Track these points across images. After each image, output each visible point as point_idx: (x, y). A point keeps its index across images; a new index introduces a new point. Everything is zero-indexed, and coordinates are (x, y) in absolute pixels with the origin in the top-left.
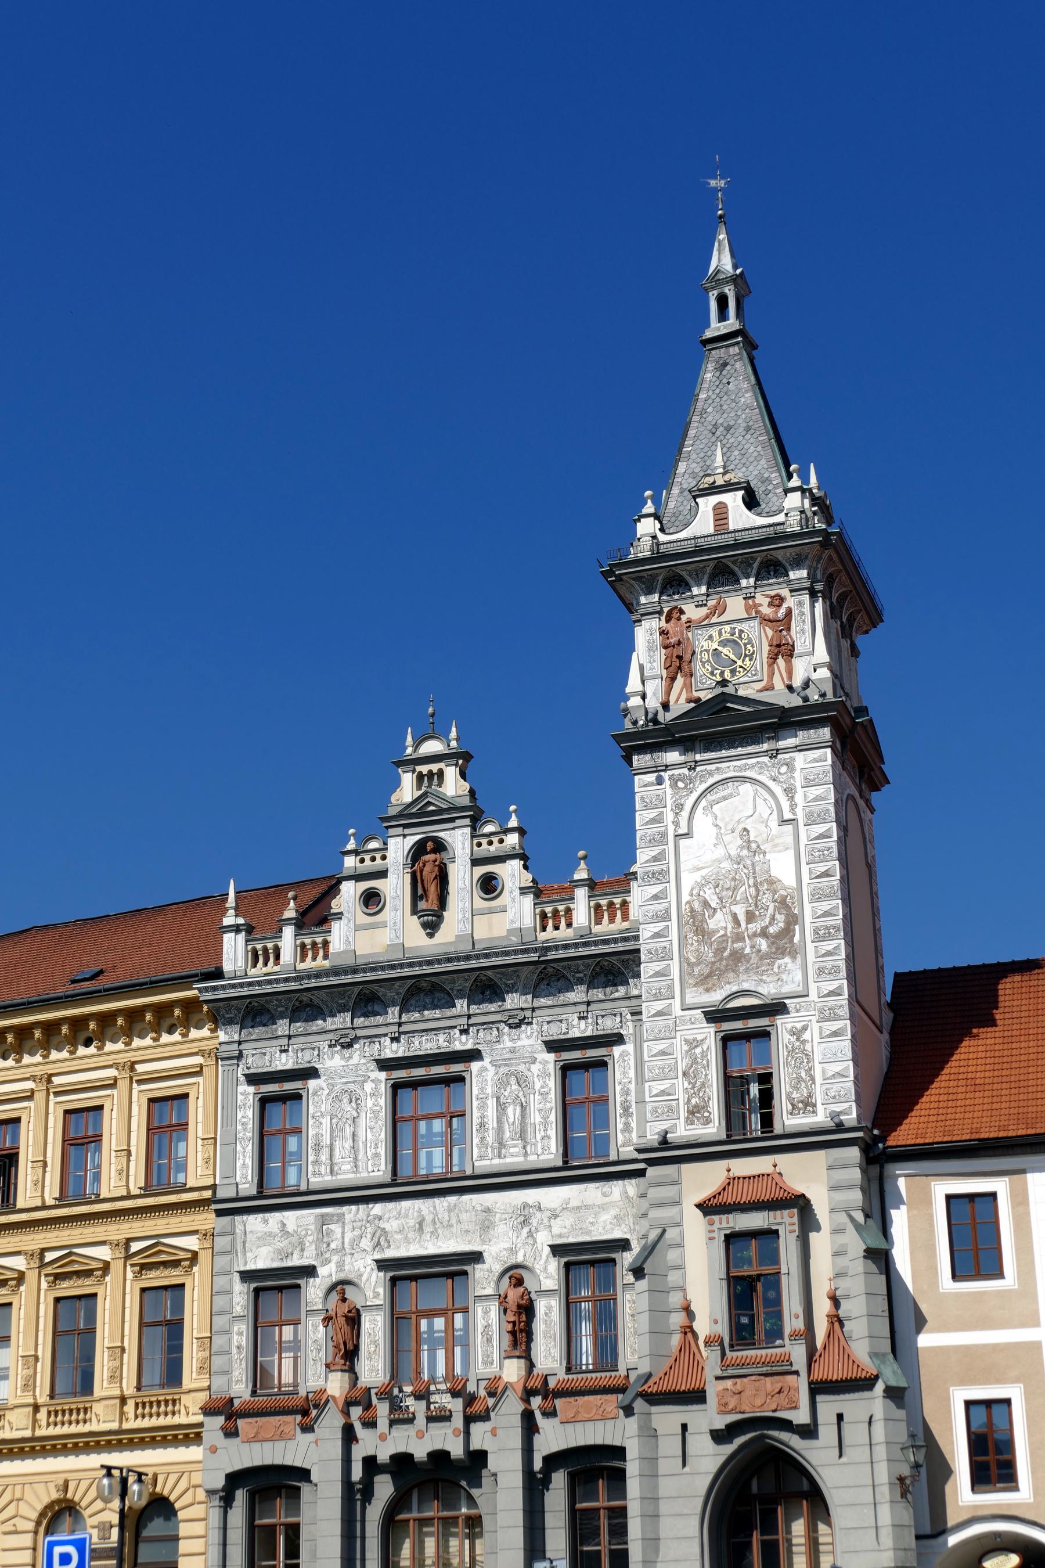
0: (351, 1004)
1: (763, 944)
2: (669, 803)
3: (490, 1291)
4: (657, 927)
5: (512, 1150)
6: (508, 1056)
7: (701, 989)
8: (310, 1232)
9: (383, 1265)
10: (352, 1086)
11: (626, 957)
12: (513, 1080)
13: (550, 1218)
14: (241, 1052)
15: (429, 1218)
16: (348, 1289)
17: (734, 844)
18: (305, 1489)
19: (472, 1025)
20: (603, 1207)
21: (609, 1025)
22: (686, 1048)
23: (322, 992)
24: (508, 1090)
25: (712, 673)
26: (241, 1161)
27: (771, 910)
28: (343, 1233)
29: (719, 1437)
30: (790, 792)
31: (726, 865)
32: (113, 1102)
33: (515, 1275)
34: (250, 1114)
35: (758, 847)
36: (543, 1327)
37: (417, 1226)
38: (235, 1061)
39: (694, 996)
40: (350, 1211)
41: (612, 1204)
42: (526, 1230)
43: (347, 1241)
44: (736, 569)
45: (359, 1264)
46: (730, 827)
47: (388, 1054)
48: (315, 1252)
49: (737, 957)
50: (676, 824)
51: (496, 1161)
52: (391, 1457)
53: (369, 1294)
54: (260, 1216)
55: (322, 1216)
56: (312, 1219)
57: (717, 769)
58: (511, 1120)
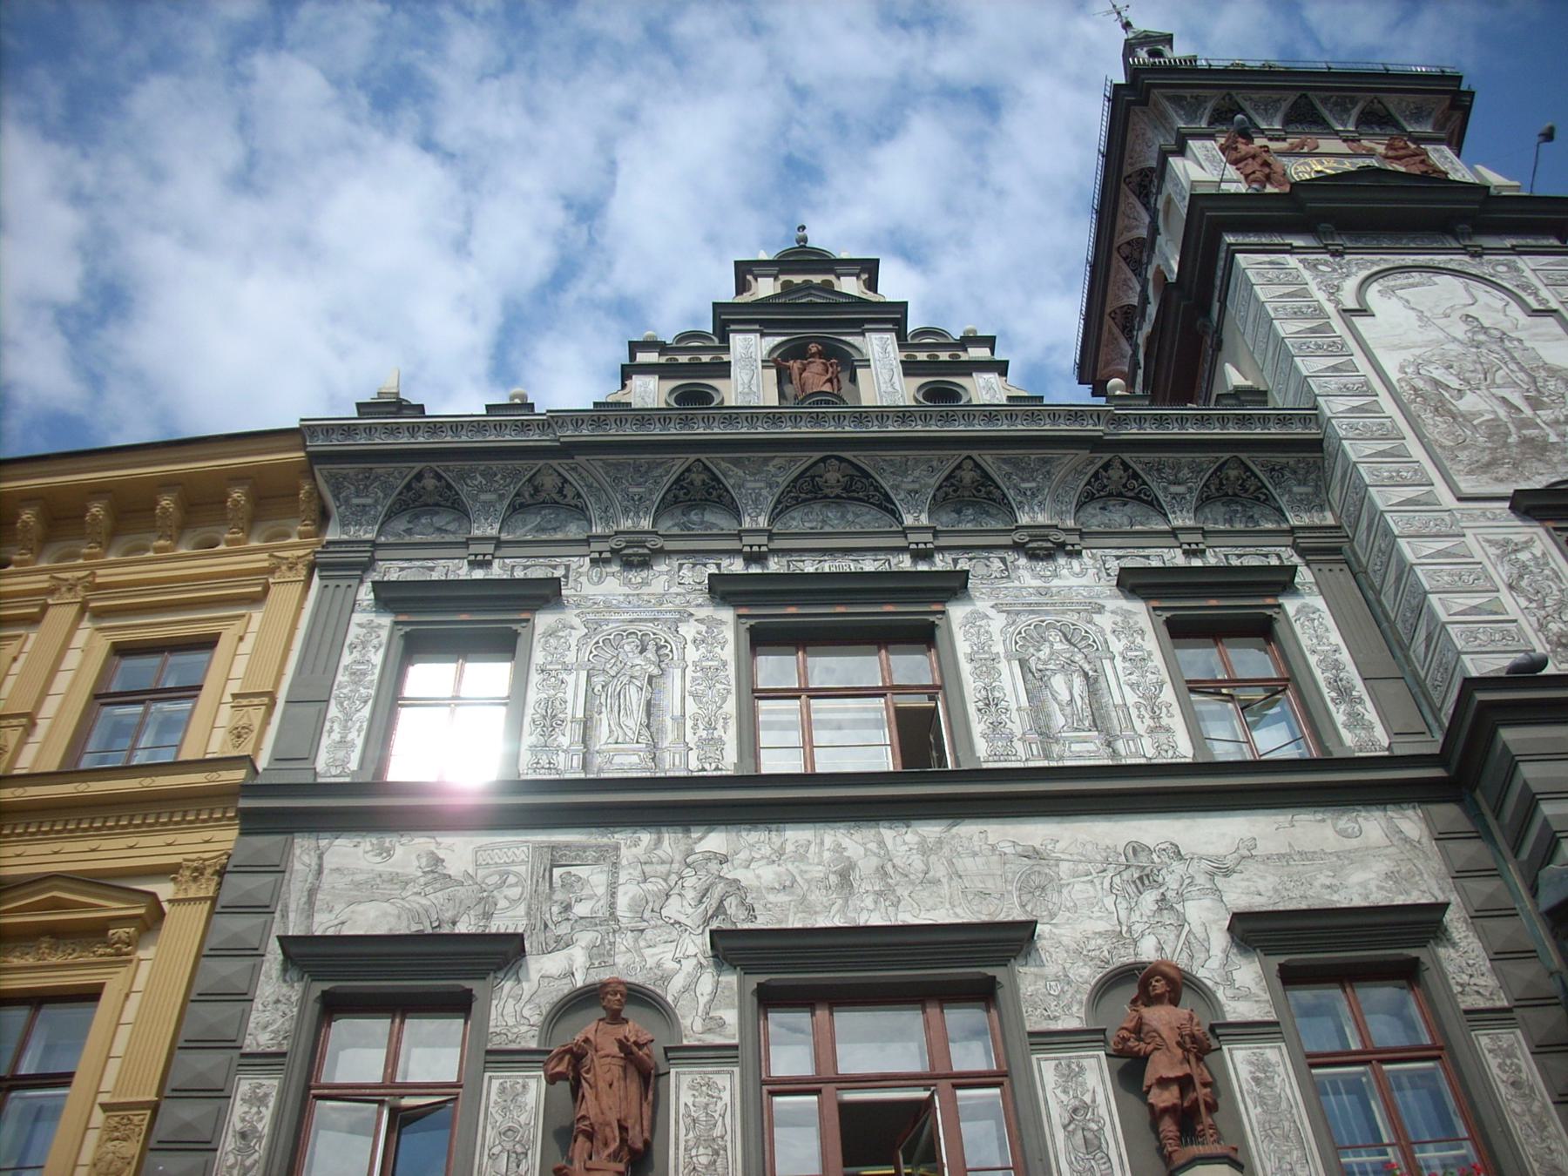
0: (657, 497)
6: (1034, 599)
7: (1485, 478)
8: (512, 879)
10: (648, 627)
11: (1280, 458)
12: (1054, 636)
13: (1212, 875)
19: (941, 549)
20: (1346, 858)
22: (1492, 551)
23: (595, 463)
26: (336, 736)
34: (377, 658)
36: (1255, 1112)
37: (833, 879)
40: (635, 844)
42: (1149, 898)
43: (623, 902)
55: (553, 848)
56: (522, 853)
58: (1065, 697)
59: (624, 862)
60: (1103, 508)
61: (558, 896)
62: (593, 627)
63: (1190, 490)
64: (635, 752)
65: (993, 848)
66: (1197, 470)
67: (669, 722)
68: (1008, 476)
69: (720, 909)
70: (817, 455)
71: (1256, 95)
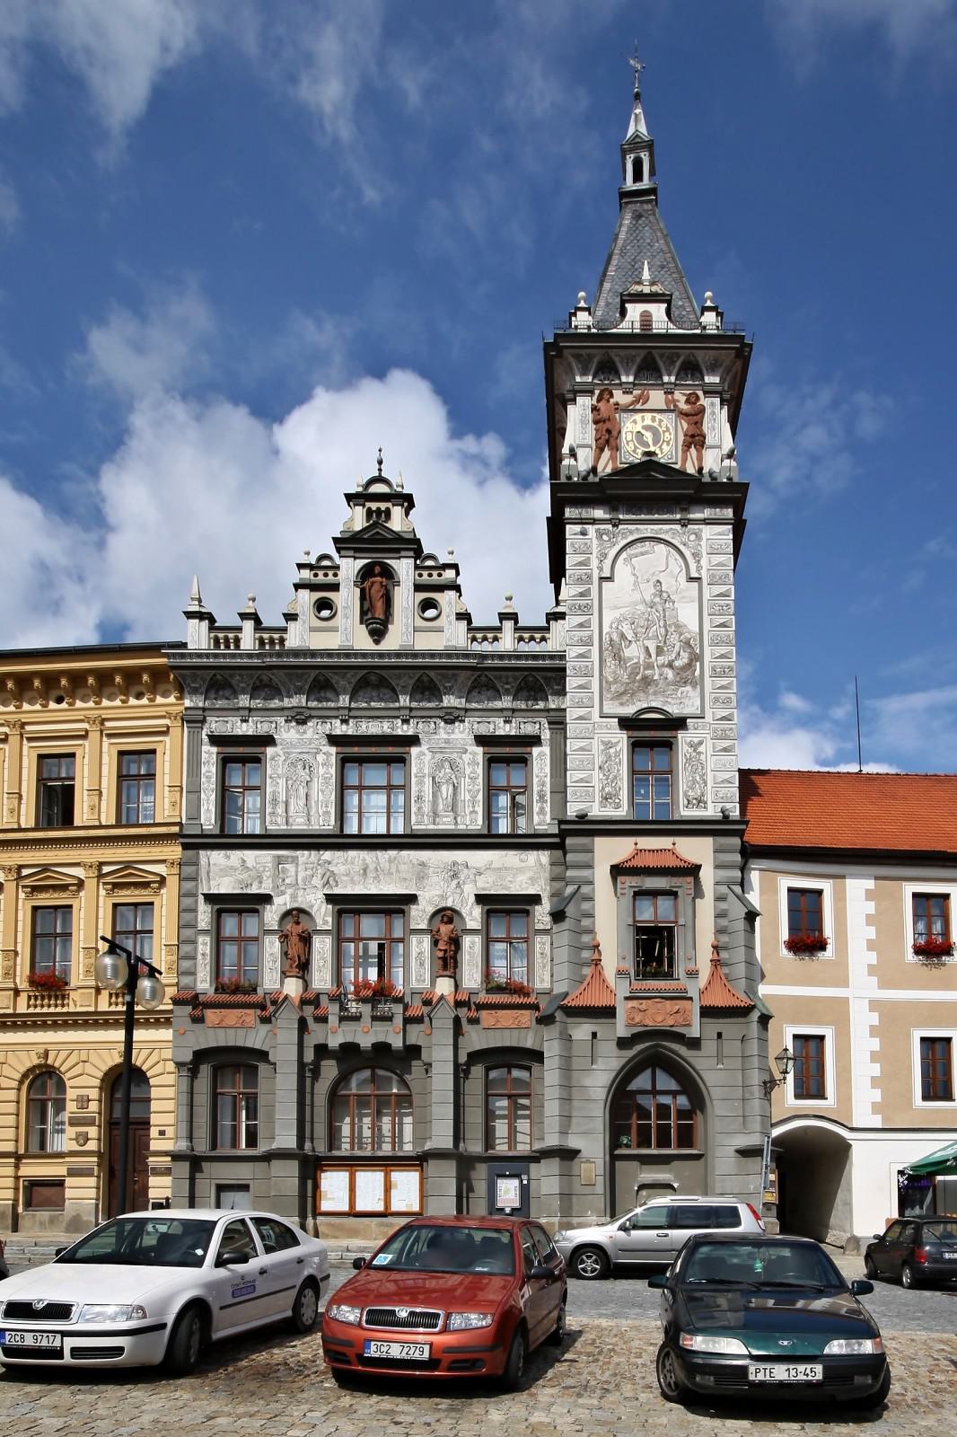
0: (307, 687)
1: (670, 674)
2: (595, 551)
3: (423, 926)
4: (582, 650)
5: (444, 819)
9: (331, 899)
11: (550, 674)
14: (205, 717)
15: (372, 867)
16: (302, 916)
17: (649, 592)
18: (263, 1068)
20: (520, 870)
23: (281, 672)
24: (443, 771)
25: (634, 451)
26: (206, 807)
27: (677, 648)
28: (297, 872)
30: (696, 555)
31: (641, 608)
32: (84, 752)
33: (446, 915)
35: (669, 596)
36: (467, 957)
37: (362, 871)
38: (200, 725)
40: (303, 855)
41: (529, 868)
42: (455, 882)
44: (661, 364)
45: (311, 898)
46: (645, 578)
48: (271, 885)
50: (601, 569)
51: (431, 827)
52: (340, 1045)
53: (319, 921)
54: (222, 853)
55: (279, 857)
56: (269, 859)
57: (637, 529)
58: (445, 796)
59: (300, 863)
60: (479, 692)
61: (281, 875)
62: (287, 754)
63: (512, 687)
64: (302, 817)
65: (411, 861)
66: (516, 679)
67: (313, 803)
68: (440, 681)
69: (328, 882)
70: (366, 671)
71: (622, 353)
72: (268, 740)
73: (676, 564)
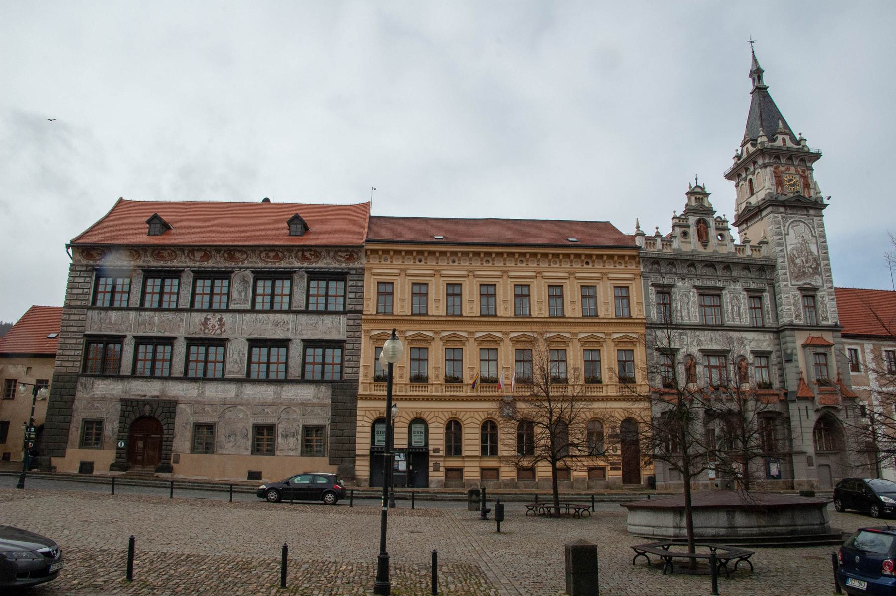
9: (701, 350)
17: (801, 240)
21: (761, 286)
29: (817, 411)
30: (814, 227)
39: (794, 282)
40: (689, 332)
47: (697, 284)
49: (804, 273)
72: (672, 286)
73: (807, 231)
